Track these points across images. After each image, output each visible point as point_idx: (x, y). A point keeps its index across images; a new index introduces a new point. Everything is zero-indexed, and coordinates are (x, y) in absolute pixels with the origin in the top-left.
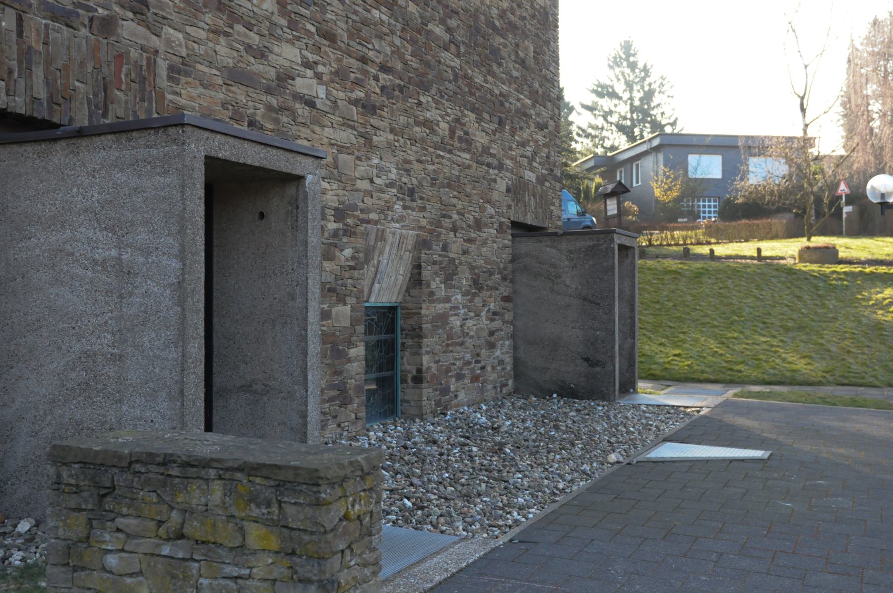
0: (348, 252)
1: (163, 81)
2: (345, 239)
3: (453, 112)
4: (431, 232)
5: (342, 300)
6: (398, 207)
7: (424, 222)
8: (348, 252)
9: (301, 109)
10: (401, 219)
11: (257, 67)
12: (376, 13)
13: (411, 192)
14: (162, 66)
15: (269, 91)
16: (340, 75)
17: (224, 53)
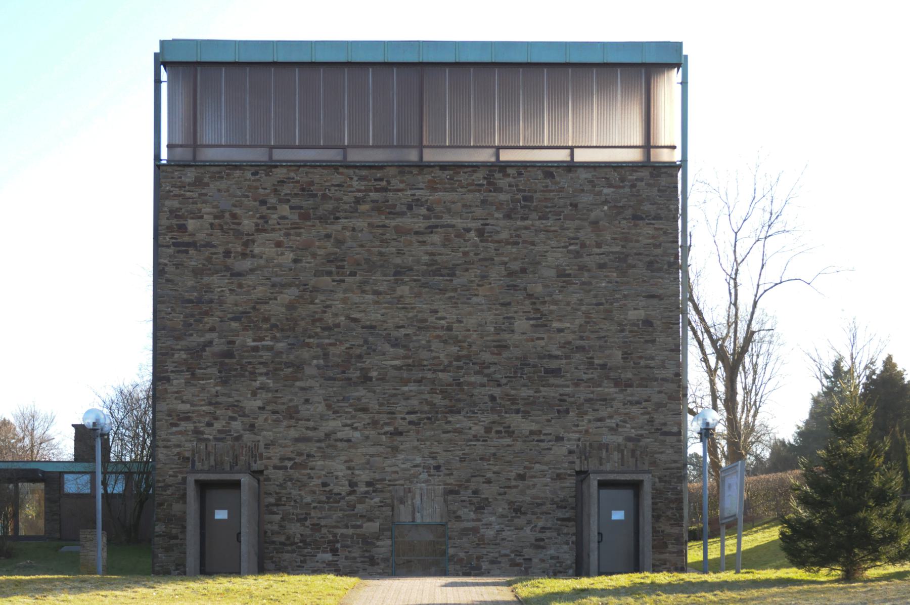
0: (377, 500)
1: (262, 449)
2: (374, 494)
3: (486, 418)
4: (460, 486)
5: (370, 520)
6: (424, 476)
7: (452, 481)
8: (377, 500)
9: (339, 444)
10: (426, 481)
11: (310, 434)
12: (406, 389)
13: (438, 468)
14: (262, 445)
15: (319, 441)
16: (375, 423)
17: (293, 433)
